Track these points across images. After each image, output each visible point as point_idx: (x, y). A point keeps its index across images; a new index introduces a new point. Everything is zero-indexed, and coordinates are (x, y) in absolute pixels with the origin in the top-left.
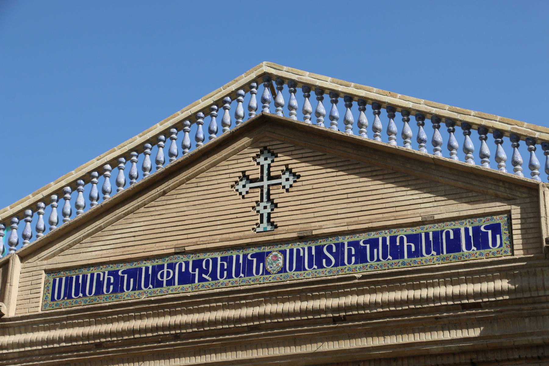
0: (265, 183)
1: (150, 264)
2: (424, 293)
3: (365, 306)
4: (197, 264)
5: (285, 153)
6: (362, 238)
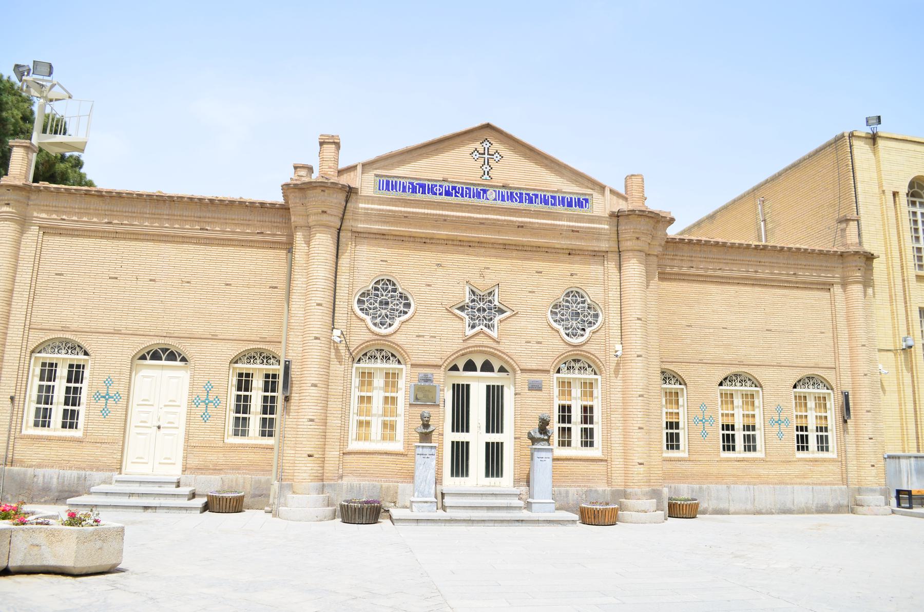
4: (454, 188)
6: (531, 193)
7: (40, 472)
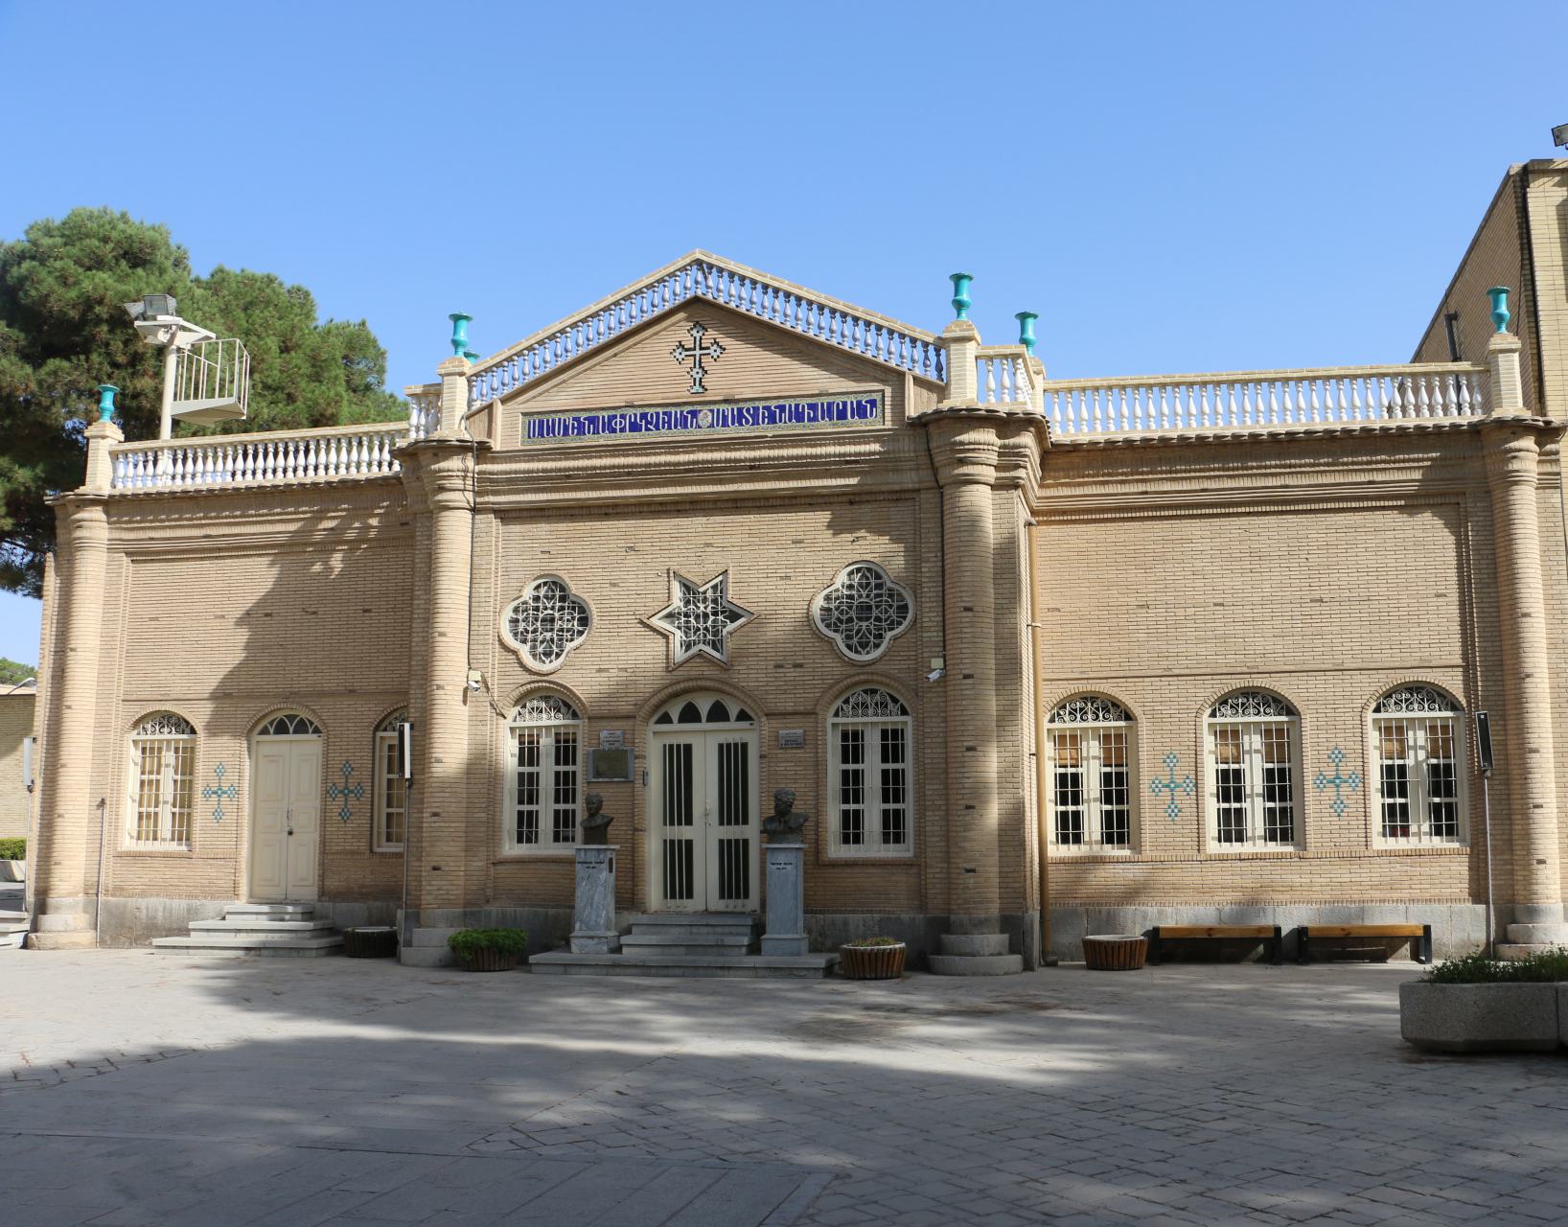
0: (698, 352)
1: (606, 414)
2: (818, 451)
3: (774, 459)
4: (644, 416)
5: (714, 328)
6: (773, 404)
7: (142, 902)
